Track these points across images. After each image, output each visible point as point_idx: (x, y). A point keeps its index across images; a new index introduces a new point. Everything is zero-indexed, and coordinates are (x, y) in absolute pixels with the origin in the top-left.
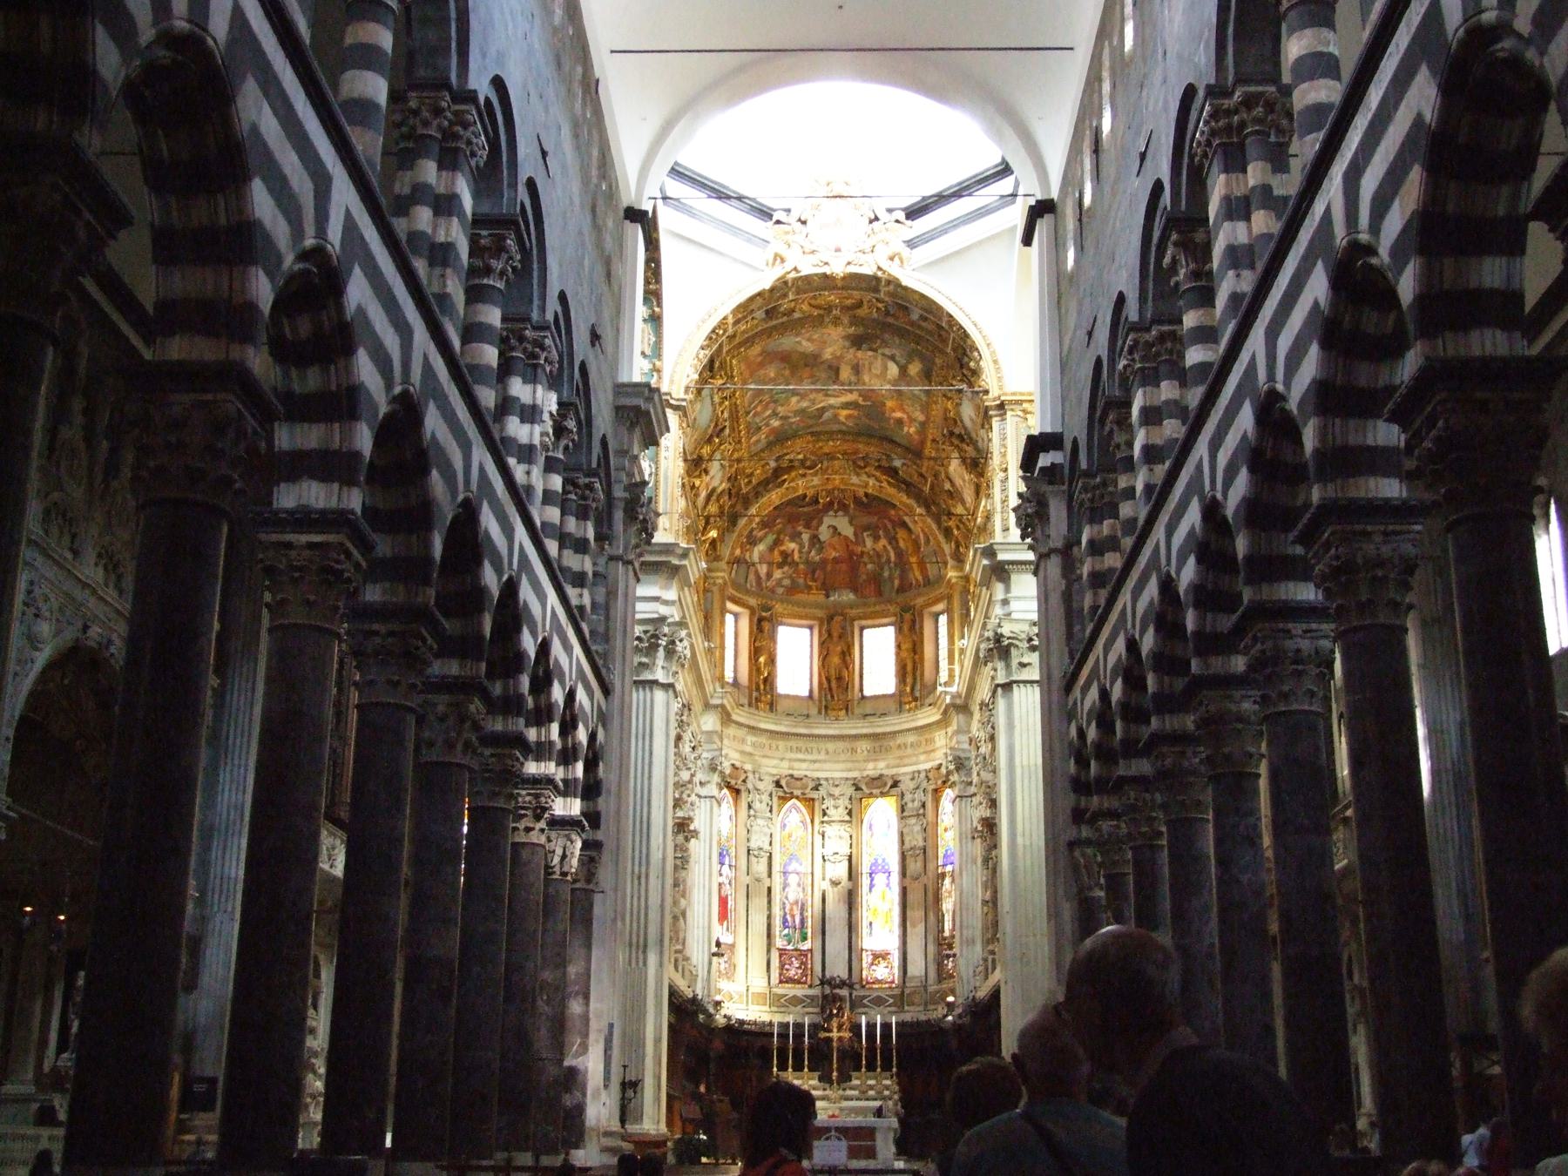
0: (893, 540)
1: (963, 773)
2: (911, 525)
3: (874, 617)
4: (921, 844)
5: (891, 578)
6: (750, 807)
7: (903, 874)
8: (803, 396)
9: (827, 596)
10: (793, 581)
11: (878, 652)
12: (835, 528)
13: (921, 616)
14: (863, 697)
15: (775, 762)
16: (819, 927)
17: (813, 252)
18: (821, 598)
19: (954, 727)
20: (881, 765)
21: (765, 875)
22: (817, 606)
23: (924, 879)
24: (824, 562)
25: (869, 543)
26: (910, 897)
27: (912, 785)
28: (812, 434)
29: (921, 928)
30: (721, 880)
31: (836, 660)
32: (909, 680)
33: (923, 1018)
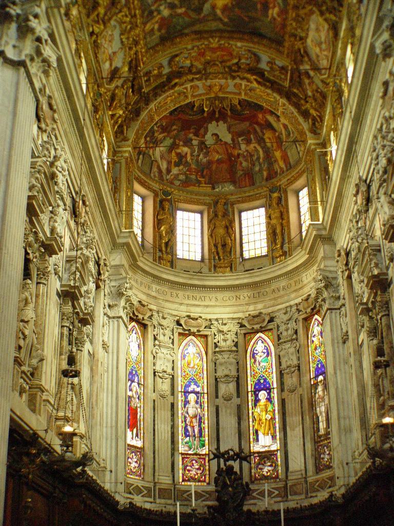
0: (261, 141)
1: (330, 290)
2: (275, 124)
3: (249, 202)
4: (295, 362)
5: (260, 171)
6: (155, 339)
7: (282, 388)
9: (213, 188)
10: (187, 177)
11: (253, 228)
12: (216, 135)
13: (286, 192)
14: (244, 260)
15: (175, 306)
16: (215, 435)
18: (208, 189)
19: (321, 254)
20: (260, 306)
21: (169, 393)
23: (300, 391)
24: (210, 163)
26: (289, 407)
27: (286, 317)
28: (196, 33)
29: (299, 430)
30: (130, 393)
31: (221, 231)
32: (279, 241)
33: (306, 503)
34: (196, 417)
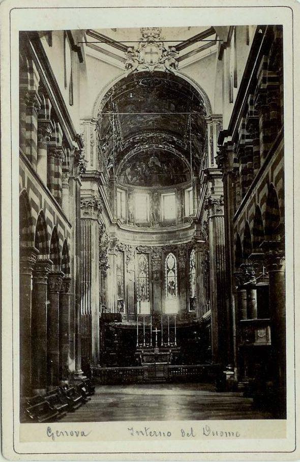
8: (142, 116)
17: (142, 63)
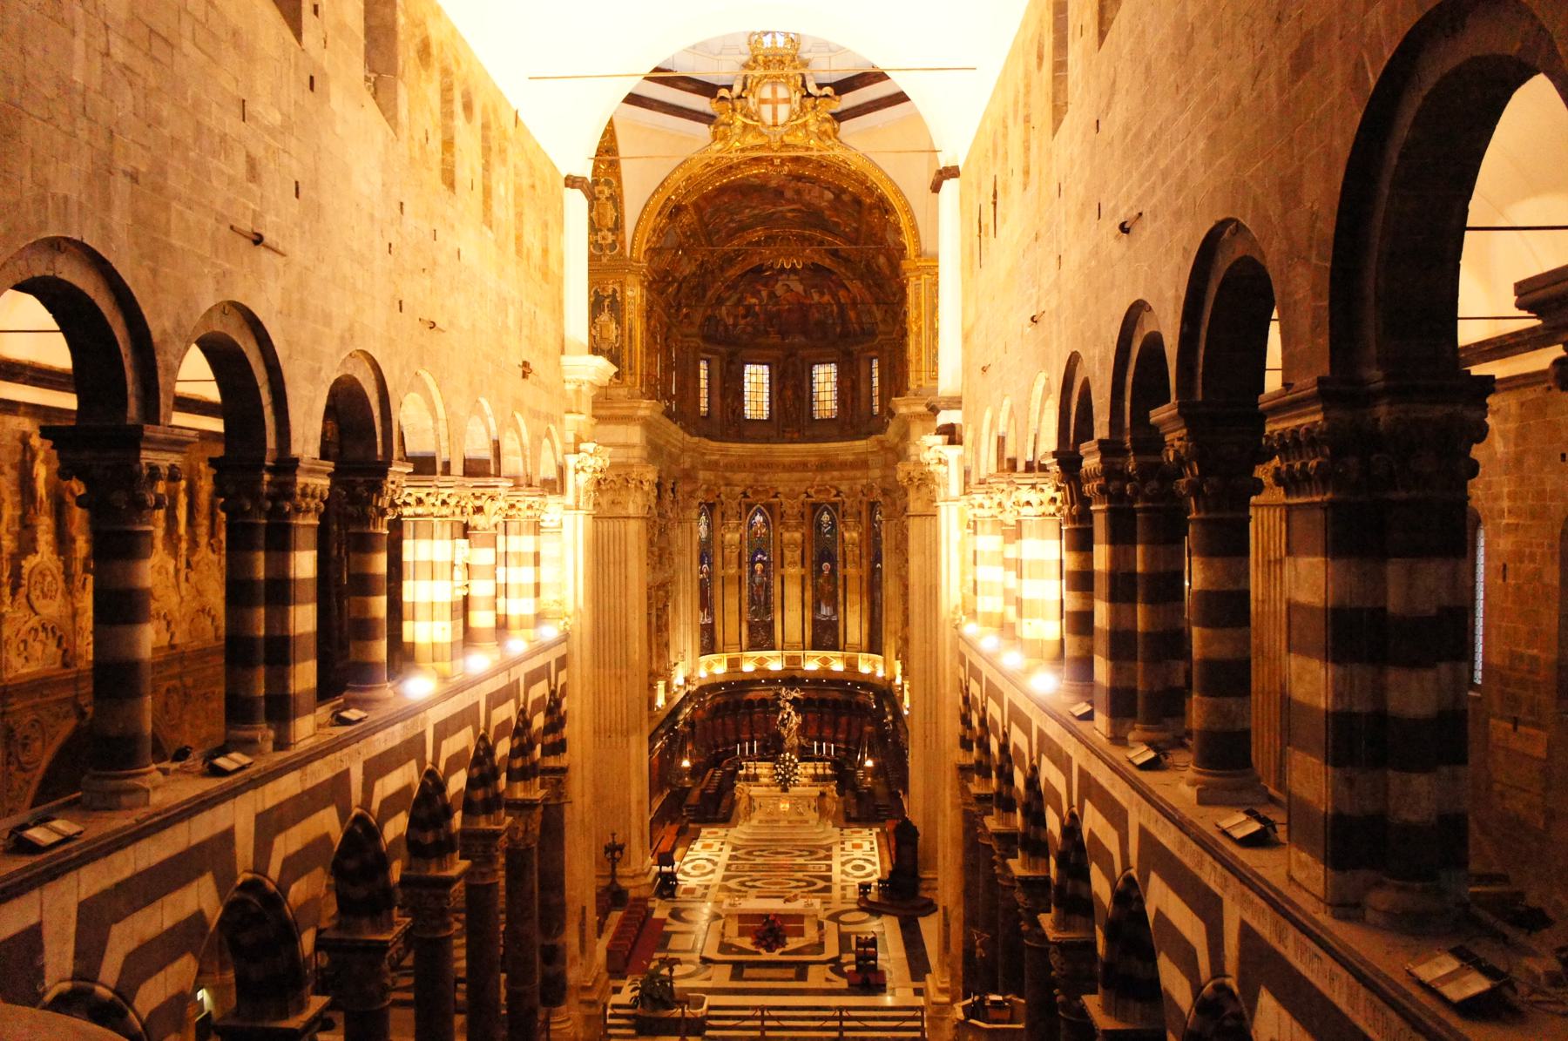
0: (834, 295)
13: (858, 359)
22: (773, 347)
25: (816, 297)
29: (857, 607)
34: (761, 585)
